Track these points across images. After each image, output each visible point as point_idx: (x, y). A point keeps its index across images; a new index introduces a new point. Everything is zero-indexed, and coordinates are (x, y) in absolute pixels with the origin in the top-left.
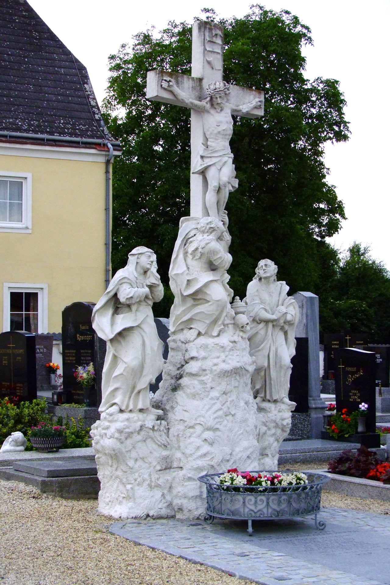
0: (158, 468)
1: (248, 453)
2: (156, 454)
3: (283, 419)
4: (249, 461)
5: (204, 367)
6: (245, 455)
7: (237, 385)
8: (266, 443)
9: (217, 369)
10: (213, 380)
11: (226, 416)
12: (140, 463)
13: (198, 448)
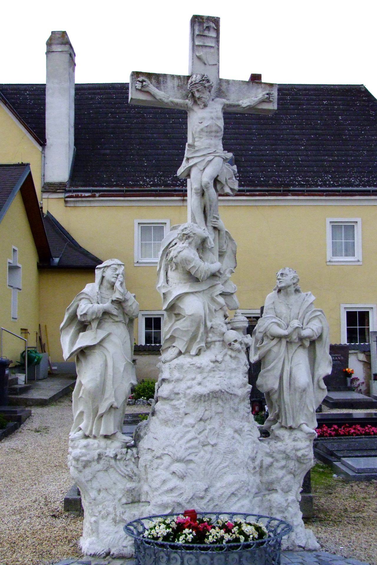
0: (124, 501)
1: (233, 489)
2: (120, 486)
3: (297, 450)
4: (235, 499)
5: (176, 390)
6: (228, 492)
7: (220, 410)
8: (273, 476)
9: (191, 392)
10: (187, 405)
11: (204, 446)
12: (103, 494)
13: (164, 482)
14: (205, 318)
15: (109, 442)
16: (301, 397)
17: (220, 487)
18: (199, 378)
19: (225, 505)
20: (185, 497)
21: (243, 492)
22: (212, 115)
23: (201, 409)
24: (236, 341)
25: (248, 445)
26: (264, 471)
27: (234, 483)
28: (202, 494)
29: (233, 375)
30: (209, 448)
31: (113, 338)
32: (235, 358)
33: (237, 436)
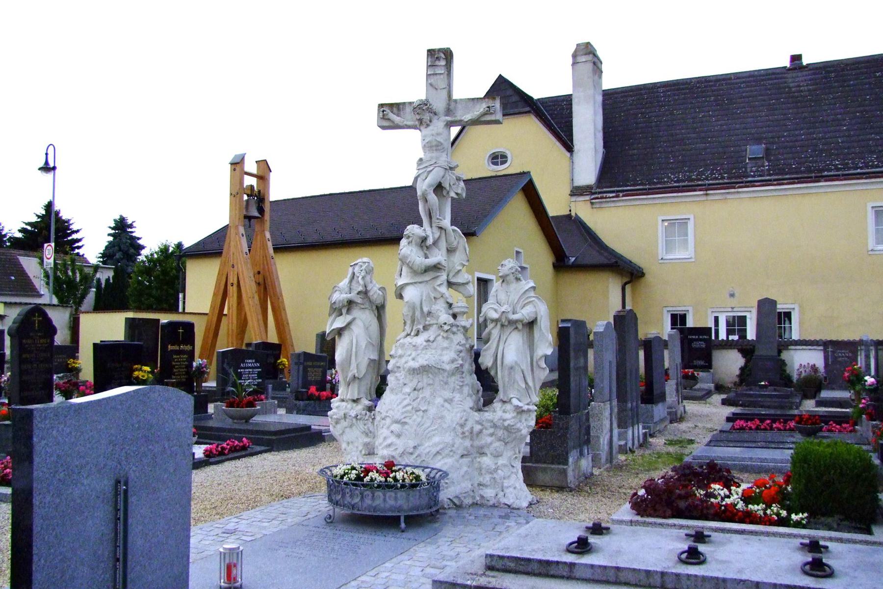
0: (363, 452)
1: (438, 449)
2: (360, 441)
3: (504, 420)
4: (440, 457)
5: (398, 365)
6: (434, 450)
7: (431, 382)
8: (483, 442)
9: (407, 366)
10: (406, 377)
11: (417, 411)
12: (351, 446)
13: (385, 438)
14: (421, 304)
15: (354, 405)
16: (510, 373)
17: (429, 447)
18: (414, 354)
19: (432, 462)
20: (398, 452)
21: (447, 452)
22: (434, 132)
23: (415, 381)
24: (445, 324)
25: (457, 413)
26: (475, 437)
27: (439, 443)
28: (411, 450)
29: (445, 352)
30: (421, 413)
31: (358, 322)
32: (447, 338)
33: (446, 404)
